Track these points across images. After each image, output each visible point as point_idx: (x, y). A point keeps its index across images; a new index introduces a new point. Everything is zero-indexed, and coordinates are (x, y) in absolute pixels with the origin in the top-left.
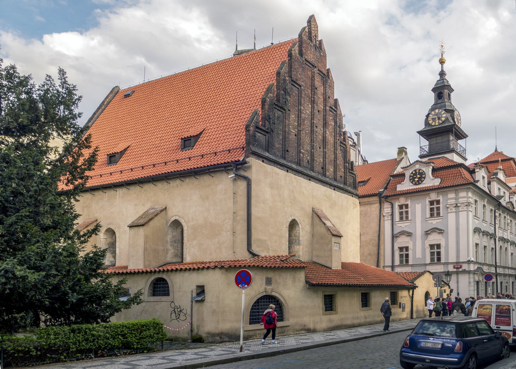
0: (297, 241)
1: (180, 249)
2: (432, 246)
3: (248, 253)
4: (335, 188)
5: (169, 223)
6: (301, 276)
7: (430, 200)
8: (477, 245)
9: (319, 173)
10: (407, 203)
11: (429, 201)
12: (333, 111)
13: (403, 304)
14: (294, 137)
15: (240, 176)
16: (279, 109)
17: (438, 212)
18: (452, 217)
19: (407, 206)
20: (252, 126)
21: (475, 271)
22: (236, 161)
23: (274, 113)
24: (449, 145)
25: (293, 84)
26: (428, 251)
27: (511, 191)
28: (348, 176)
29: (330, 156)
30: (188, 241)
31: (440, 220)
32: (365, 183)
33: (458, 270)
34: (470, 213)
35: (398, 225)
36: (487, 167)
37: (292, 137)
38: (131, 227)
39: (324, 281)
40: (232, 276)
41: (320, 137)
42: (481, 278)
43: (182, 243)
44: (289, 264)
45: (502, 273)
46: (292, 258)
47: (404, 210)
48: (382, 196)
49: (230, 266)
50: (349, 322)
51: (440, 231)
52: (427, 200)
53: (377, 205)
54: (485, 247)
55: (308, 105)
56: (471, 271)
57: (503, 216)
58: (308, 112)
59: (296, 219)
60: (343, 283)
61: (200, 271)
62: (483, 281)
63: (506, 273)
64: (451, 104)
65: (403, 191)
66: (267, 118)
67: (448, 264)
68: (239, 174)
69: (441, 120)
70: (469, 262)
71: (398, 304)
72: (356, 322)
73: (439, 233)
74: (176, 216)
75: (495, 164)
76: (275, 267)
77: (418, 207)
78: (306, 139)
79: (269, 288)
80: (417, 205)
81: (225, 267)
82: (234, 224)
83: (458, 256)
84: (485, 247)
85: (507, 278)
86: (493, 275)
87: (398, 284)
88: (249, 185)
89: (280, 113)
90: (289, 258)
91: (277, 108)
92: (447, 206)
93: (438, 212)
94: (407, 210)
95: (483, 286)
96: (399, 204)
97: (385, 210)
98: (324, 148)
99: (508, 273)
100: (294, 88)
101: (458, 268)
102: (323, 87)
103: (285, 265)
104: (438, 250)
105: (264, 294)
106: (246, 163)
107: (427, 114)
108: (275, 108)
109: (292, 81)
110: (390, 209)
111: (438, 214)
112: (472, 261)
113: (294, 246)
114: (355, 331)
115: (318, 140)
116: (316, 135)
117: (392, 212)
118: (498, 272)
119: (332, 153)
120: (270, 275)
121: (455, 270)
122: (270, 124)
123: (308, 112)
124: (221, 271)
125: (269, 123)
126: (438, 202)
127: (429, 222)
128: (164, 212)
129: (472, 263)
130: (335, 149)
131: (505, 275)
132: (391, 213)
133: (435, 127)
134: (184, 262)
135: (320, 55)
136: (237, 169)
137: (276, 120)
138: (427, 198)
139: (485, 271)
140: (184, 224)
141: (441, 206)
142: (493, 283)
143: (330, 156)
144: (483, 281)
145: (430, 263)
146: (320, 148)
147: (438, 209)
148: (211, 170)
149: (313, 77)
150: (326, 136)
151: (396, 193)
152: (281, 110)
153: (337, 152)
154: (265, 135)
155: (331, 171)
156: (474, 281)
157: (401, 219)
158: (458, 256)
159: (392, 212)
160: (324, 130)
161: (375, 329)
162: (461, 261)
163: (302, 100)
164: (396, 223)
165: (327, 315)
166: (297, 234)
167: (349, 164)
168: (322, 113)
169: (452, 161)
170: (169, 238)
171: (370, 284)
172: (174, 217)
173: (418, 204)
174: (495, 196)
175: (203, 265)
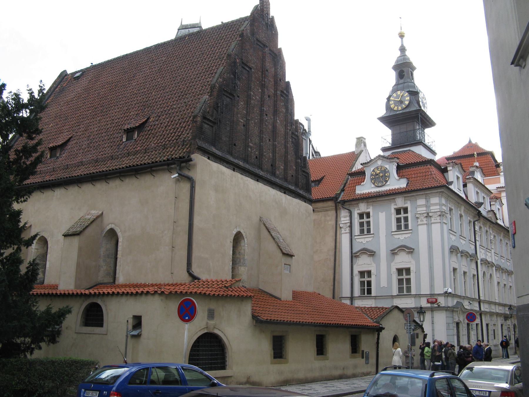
0: (242, 261)
1: (112, 265)
2: (400, 271)
3: (187, 274)
4: (286, 190)
5: (104, 233)
6: (247, 308)
7: (396, 207)
8: (455, 270)
9: (267, 171)
10: (368, 210)
11: (395, 209)
12: (284, 96)
13: (366, 352)
14: (242, 128)
15: (183, 176)
16: (228, 95)
17: (406, 223)
18: (422, 230)
19: (368, 215)
20: (199, 117)
21: (453, 307)
22: (180, 158)
23: (223, 101)
24: (415, 136)
25: (244, 66)
26: (395, 278)
27: (492, 195)
28: (301, 176)
29: (281, 150)
30: (122, 256)
31: (409, 235)
32: (317, 183)
33: (432, 305)
34: (445, 227)
35: (358, 240)
36: (461, 164)
37: (241, 128)
38: (66, 236)
39: (273, 316)
40: (174, 306)
41: (270, 127)
42: (462, 318)
43: (116, 259)
44: (234, 292)
45: (488, 310)
46: (237, 284)
47: (365, 220)
48: (339, 201)
49: (171, 292)
50: (301, 375)
51: (410, 251)
52: (393, 207)
53: (333, 213)
54: (465, 273)
55: (258, 89)
56: (449, 307)
57: (484, 230)
58: (258, 98)
59: (242, 231)
60: (295, 320)
61: (138, 297)
62: (464, 323)
63: (492, 311)
64: (415, 84)
65: (363, 194)
66: (216, 107)
68: (183, 174)
69: (405, 104)
70: (447, 294)
71: (361, 352)
72: (310, 375)
74: (112, 224)
75: (470, 159)
76: (219, 295)
77: (382, 217)
78: (254, 130)
79: (211, 322)
80: (380, 213)
81: (165, 292)
82: (174, 236)
83: (432, 286)
84: (465, 273)
85: (494, 318)
86: (476, 313)
87: (360, 324)
88: (193, 187)
89: (228, 99)
90: (234, 283)
91: (226, 94)
92: (417, 216)
93: (406, 223)
94: (368, 220)
95: (464, 330)
96: (359, 212)
97: (342, 219)
98: (274, 140)
99: (494, 311)
100: (244, 71)
101: (432, 303)
102: (273, 69)
103: (230, 293)
104: (408, 277)
105: (206, 331)
106: (191, 160)
107: (387, 96)
108: (223, 94)
109: (243, 63)
110: (348, 218)
111: (406, 226)
113: (238, 267)
114: (309, 388)
115: (268, 130)
116: (266, 125)
117: (351, 223)
118: (482, 309)
119: (283, 146)
120: (213, 305)
121: (429, 305)
122: (218, 113)
123: (258, 98)
124: (161, 298)
125: (217, 111)
126: (406, 210)
128: (99, 219)
129: (450, 296)
130: (286, 142)
131: (491, 314)
132: (349, 224)
133: (398, 112)
134: (117, 283)
135: (272, 34)
136: (181, 168)
137: (224, 109)
138: (393, 204)
139: (466, 307)
140: (119, 234)
141: (409, 215)
142: (477, 325)
143: (281, 150)
144: (464, 323)
145: (398, 295)
146: (269, 140)
147: (406, 219)
148: (153, 169)
149: (264, 57)
150: (276, 126)
151: (355, 197)
152: (230, 97)
153: (289, 145)
154: (212, 127)
155: (282, 169)
157: (362, 231)
158: (432, 286)
159: (351, 223)
160: (274, 119)
161: (333, 387)
162: (436, 293)
163: (253, 84)
164: (356, 237)
165: (275, 363)
166: (242, 251)
167: (301, 160)
168: (273, 98)
169: (419, 156)
170: (102, 251)
171: (327, 322)
172: (110, 225)
173: (382, 212)
174: (473, 202)
175: (141, 290)
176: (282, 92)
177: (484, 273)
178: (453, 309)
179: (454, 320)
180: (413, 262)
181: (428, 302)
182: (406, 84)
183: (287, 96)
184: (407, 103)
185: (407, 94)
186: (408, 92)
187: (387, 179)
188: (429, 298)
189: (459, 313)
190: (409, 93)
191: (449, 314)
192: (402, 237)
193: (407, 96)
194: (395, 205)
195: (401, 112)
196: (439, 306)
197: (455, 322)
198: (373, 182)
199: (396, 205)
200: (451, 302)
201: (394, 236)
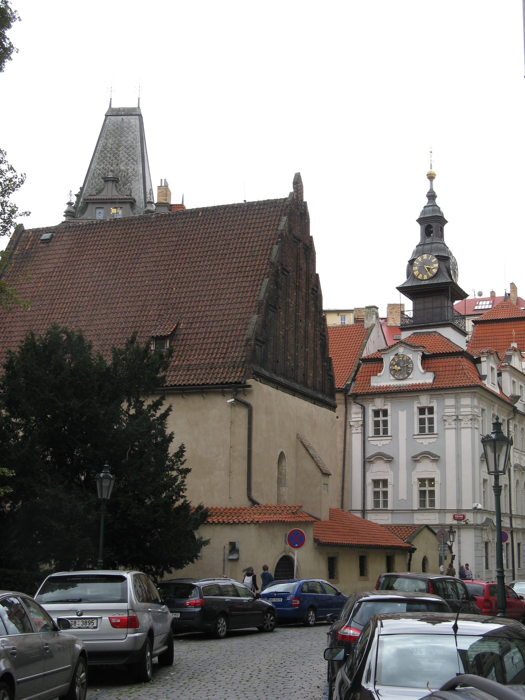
2: (422, 481)
7: (419, 406)
21: (483, 525)
33: (460, 522)
67: (445, 513)
73: (434, 461)
101: (459, 520)
111: (431, 429)
112: (480, 509)
118: (514, 526)
121: (455, 522)
127: (418, 441)
156: (483, 542)
176: (313, 289)
177: (517, 481)
178: (482, 527)
179: (483, 540)
180: (438, 472)
181: (454, 518)
182: (434, 245)
183: (316, 292)
184: (435, 271)
185: (435, 259)
186: (436, 256)
187: (409, 371)
188: (456, 513)
189: (488, 531)
190: (438, 259)
191: (478, 533)
192: (426, 442)
193: (435, 263)
194: (418, 403)
195: (427, 282)
196: (467, 523)
197: (484, 542)
198: (393, 373)
199: (420, 403)
200: (480, 519)
201: (416, 440)
